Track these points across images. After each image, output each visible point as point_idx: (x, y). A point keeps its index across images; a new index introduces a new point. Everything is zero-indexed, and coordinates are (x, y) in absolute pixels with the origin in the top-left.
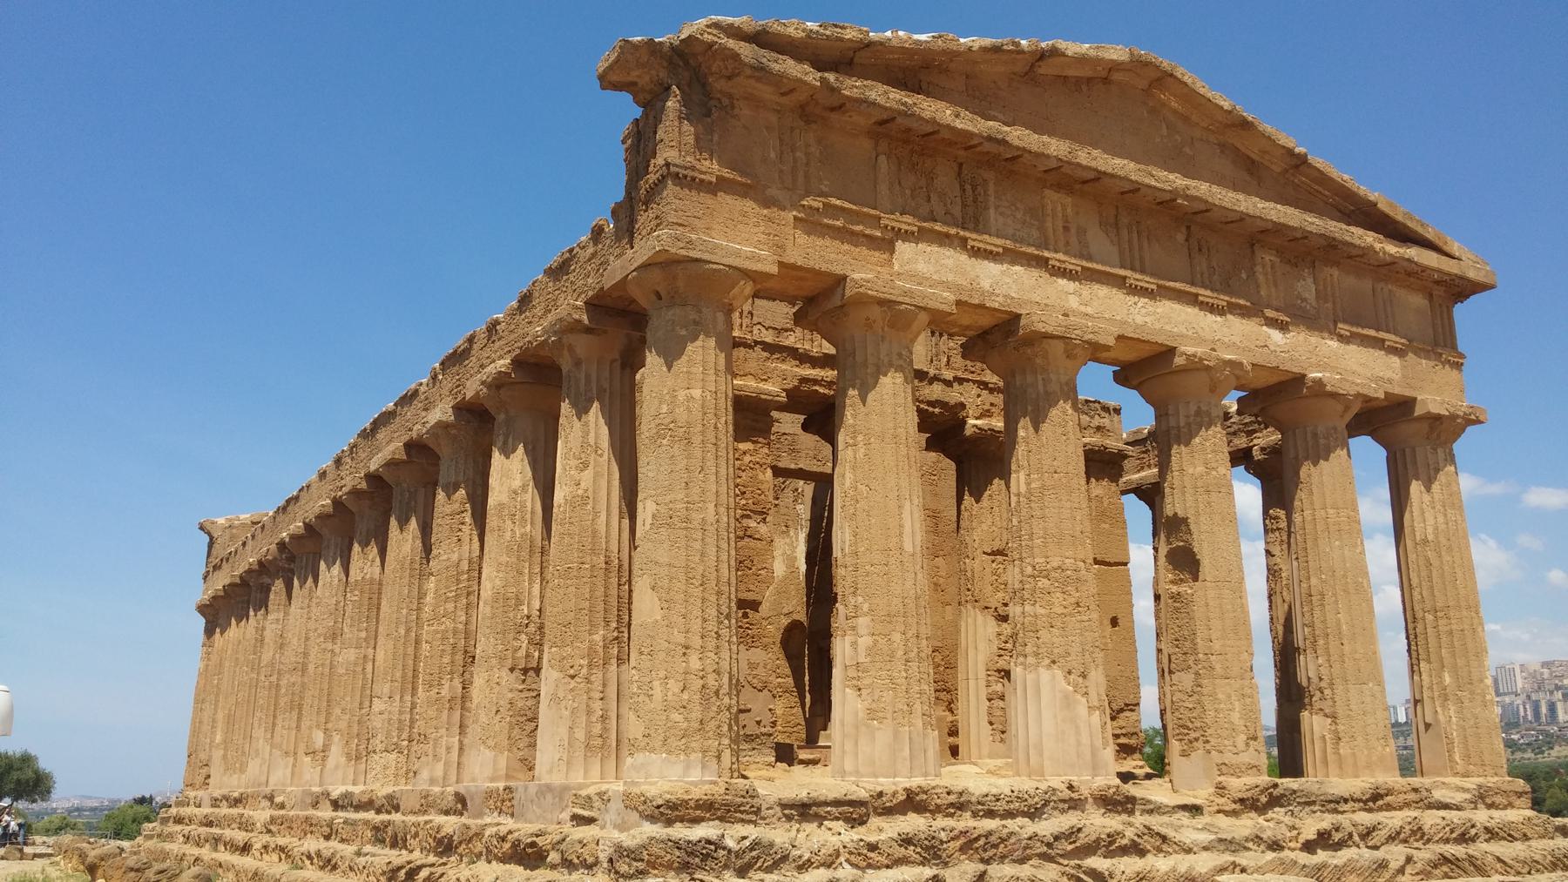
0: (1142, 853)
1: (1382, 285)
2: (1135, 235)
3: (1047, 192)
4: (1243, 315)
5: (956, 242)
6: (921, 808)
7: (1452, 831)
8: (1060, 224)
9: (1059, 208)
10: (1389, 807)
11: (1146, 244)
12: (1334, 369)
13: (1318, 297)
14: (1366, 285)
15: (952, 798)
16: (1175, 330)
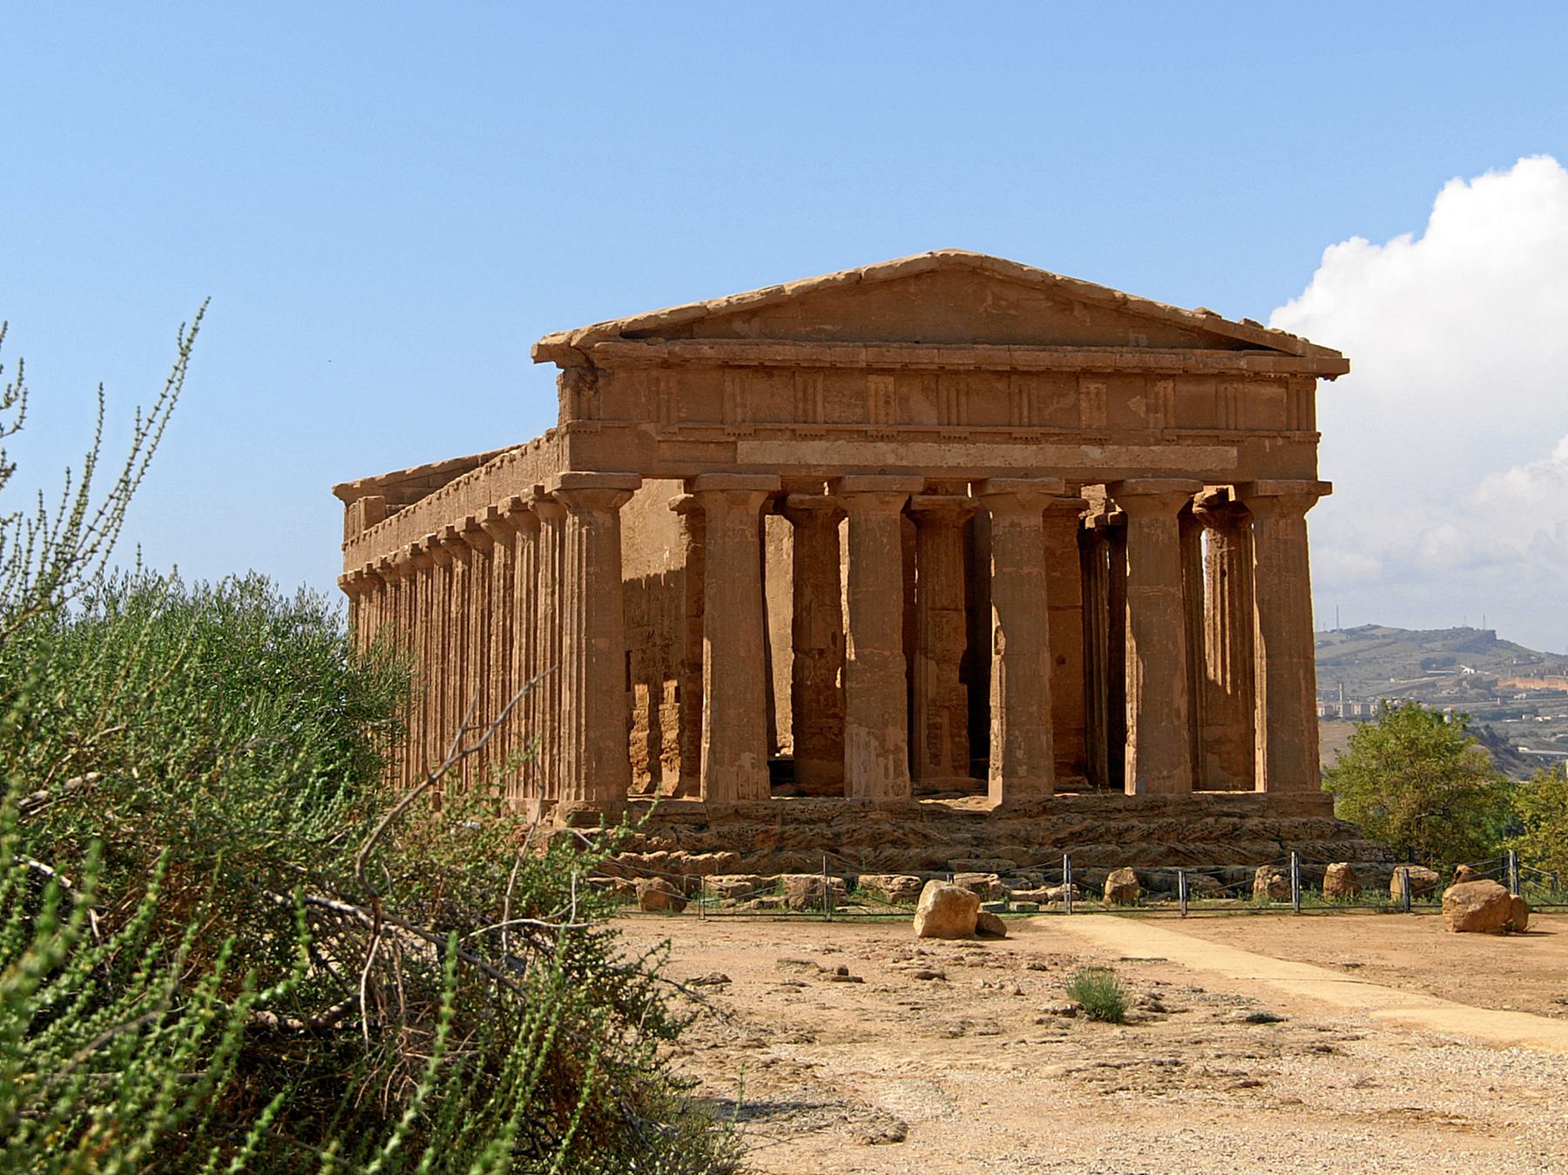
0: (908, 846)
1: (1227, 385)
2: (953, 396)
3: (872, 378)
4: (1059, 442)
5: (788, 433)
6: (747, 817)
7: (1211, 833)
8: (882, 400)
9: (882, 386)
10: (1164, 815)
11: (963, 399)
12: (1156, 473)
13: (1148, 411)
14: (1209, 388)
15: (768, 811)
16: (988, 464)
